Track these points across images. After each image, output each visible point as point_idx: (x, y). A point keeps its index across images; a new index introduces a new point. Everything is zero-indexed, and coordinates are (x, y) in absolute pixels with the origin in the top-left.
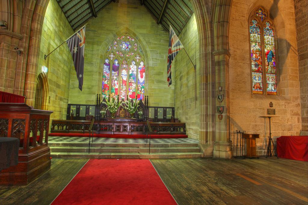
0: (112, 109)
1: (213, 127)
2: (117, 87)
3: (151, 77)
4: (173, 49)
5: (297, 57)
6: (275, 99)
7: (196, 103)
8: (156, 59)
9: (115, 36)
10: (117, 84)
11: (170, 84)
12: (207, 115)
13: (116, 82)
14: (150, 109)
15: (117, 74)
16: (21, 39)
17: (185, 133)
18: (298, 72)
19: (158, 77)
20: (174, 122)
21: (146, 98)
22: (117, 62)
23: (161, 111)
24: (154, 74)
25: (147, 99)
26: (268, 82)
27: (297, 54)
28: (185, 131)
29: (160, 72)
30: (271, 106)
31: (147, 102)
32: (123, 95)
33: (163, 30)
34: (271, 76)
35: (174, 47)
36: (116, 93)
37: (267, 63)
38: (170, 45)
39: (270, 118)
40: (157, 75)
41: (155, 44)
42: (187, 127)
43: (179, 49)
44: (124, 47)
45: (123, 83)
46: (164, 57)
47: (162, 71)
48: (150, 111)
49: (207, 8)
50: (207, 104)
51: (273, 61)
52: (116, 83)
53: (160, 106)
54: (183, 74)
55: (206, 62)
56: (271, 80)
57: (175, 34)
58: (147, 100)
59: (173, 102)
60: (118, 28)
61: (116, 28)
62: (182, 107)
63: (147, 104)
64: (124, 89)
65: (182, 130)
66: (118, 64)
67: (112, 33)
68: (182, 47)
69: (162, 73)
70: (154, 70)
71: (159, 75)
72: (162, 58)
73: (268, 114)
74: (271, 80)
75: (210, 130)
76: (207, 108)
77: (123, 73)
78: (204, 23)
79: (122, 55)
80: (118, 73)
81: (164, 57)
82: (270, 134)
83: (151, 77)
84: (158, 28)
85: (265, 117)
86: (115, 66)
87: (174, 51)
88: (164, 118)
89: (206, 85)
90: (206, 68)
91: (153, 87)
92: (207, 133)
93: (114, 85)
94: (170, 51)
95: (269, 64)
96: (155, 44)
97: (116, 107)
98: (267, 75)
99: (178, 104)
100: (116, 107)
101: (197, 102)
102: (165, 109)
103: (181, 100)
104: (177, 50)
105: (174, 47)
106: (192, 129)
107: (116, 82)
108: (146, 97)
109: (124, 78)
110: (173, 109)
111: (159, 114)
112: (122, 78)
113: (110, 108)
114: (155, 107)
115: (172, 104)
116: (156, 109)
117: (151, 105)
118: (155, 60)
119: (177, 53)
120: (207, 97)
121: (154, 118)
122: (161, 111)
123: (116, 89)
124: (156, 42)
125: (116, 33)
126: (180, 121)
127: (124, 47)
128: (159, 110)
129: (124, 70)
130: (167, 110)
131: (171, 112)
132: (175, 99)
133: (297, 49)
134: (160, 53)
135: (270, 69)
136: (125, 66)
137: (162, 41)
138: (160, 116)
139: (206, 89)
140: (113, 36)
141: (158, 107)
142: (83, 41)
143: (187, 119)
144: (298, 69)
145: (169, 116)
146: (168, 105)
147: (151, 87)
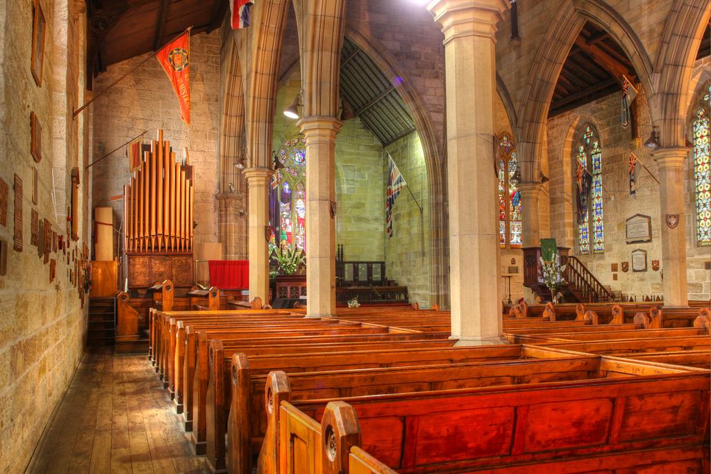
0: (289, 267)
1: (445, 290)
2: (290, 229)
3: (346, 212)
4: (394, 188)
5: (549, 200)
6: (516, 254)
7: (423, 260)
8: (353, 180)
9: (283, 141)
10: (290, 224)
11: (391, 236)
12: (438, 276)
13: (287, 221)
14: (346, 265)
15: (288, 208)
16: (241, 200)
17: (408, 302)
18: (549, 219)
19: (356, 212)
20: (389, 285)
21: (340, 247)
22: (287, 187)
23: (363, 269)
24: (351, 208)
25: (342, 249)
26: (513, 232)
27: (548, 195)
28: (407, 298)
29: (359, 203)
30: (513, 264)
31: (342, 255)
32: (300, 243)
33: (363, 128)
34: (516, 224)
35: (395, 185)
36: (289, 241)
37: (511, 208)
38: (390, 184)
39: (509, 277)
40: (355, 208)
41: (351, 154)
42: (410, 292)
43: (401, 187)
44: (297, 159)
45: (299, 223)
46: (367, 177)
47: (364, 202)
48: (346, 269)
49: (438, 147)
50: (437, 263)
51: (519, 204)
52: (288, 223)
53: (361, 260)
54: (402, 212)
55: (437, 214)
56: (516, 229)
57: (395, 166)
58: (342, 252)
59: (383, 253)
60: (288, 126)
61: (284, 126)
62: (401, 263)
63: (342, 257)
64: (301, 233)
65: (403, 297)
66: (289, 190)
67: (280, 136)
68: (404, 184)
69: (364, 204)
70: (350, 200)
71: (358, 208)
72: (362, 178)
73: (510, 272)
74: (516, 229)
75: (442, 292)
76: (438, 268)
77: (298, 206)
78: (434, 164)
79: (296, 174)
80: (291, 206)
81: (367, 177)
82: (510, 295)
83: (346, 212)
84: (354, 124)
85: (505, 277)
86: (285, 194)
87: (395, 191)
88: (368, 279)
89: (437, 241)
90: (437, 218)
91: (349, 230)
92: (438, 296)
93: (286, 227)
94: (390, 192)
95: (514, 209)
96: (351, 154)
97: (295, 265)
98: (511, 223)
99: (392, 257)
100: (295, 265)
101: (424, 258)
102: (370, 264)
103: (399, 252)
104: (398, 189)
105: (395, 185)
106: (419, 294)
107: (287, 221)
108: (339, 245)
109: (300, 215)
110: (383, 264)
111: (360, 273)
112: (298, 214)
113: (285, 266)
114: (354, 263)
115: (380, 256)
116: (356, 265)
117: (348, 260)
118: (352, 182)
119: (398, 193)
120: (437, 254)
121: (352, 280)
122: (363, 269)
123: (289, 234)
124: (353, 151)
125: (286, 136)
126: (396, 285)
127: (297, 159)
128: (360, 267)
129: (300, 200)
130: (374, 266)
131: (379, 270)
132: (386, 249)
133: (548, 189)
134: (359, 170)
135: (515, 216)
136: (300, 193)
137: (362, 147)
138: (363, 277)
139: (437, 246)
140: (280, 142)
141: (359, 263)
142: (276, 180)
143: (409, 280)
144: (549, 214)
145: (377, 276)
146: (374, 257)
147: (346, 229)
